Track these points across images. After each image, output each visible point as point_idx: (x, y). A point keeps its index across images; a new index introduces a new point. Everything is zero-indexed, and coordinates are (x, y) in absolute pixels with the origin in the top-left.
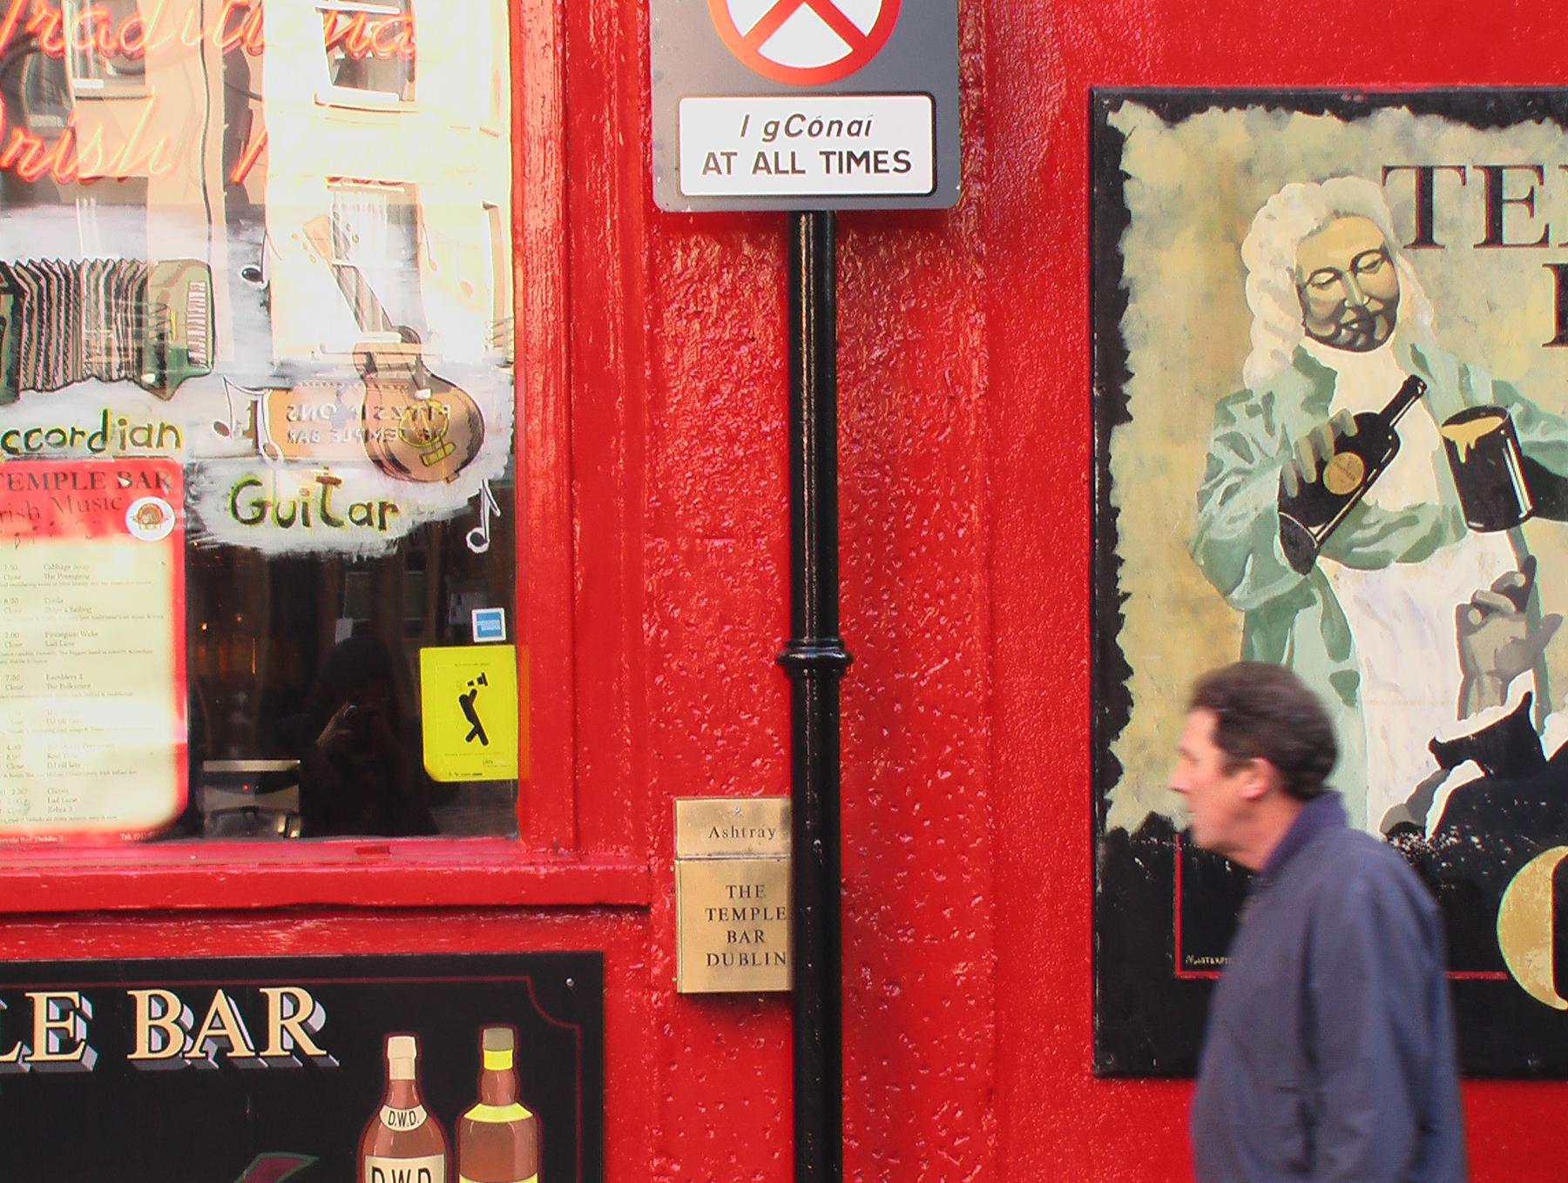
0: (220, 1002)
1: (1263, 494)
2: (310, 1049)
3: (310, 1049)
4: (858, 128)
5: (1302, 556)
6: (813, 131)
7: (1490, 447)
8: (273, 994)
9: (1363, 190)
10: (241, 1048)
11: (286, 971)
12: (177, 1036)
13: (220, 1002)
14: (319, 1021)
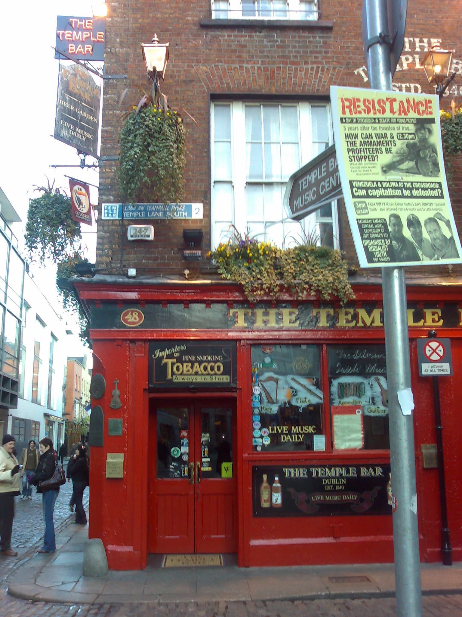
0: (371, 469)
2: (381, 474)
3: (381, 474)
4: (441, 367)
6: (437, 367)
8: (376, 468)
10: (373, 474)
11: (378, 465)
12: (366, 473)
13: (371, 469)
14: (382, 471)
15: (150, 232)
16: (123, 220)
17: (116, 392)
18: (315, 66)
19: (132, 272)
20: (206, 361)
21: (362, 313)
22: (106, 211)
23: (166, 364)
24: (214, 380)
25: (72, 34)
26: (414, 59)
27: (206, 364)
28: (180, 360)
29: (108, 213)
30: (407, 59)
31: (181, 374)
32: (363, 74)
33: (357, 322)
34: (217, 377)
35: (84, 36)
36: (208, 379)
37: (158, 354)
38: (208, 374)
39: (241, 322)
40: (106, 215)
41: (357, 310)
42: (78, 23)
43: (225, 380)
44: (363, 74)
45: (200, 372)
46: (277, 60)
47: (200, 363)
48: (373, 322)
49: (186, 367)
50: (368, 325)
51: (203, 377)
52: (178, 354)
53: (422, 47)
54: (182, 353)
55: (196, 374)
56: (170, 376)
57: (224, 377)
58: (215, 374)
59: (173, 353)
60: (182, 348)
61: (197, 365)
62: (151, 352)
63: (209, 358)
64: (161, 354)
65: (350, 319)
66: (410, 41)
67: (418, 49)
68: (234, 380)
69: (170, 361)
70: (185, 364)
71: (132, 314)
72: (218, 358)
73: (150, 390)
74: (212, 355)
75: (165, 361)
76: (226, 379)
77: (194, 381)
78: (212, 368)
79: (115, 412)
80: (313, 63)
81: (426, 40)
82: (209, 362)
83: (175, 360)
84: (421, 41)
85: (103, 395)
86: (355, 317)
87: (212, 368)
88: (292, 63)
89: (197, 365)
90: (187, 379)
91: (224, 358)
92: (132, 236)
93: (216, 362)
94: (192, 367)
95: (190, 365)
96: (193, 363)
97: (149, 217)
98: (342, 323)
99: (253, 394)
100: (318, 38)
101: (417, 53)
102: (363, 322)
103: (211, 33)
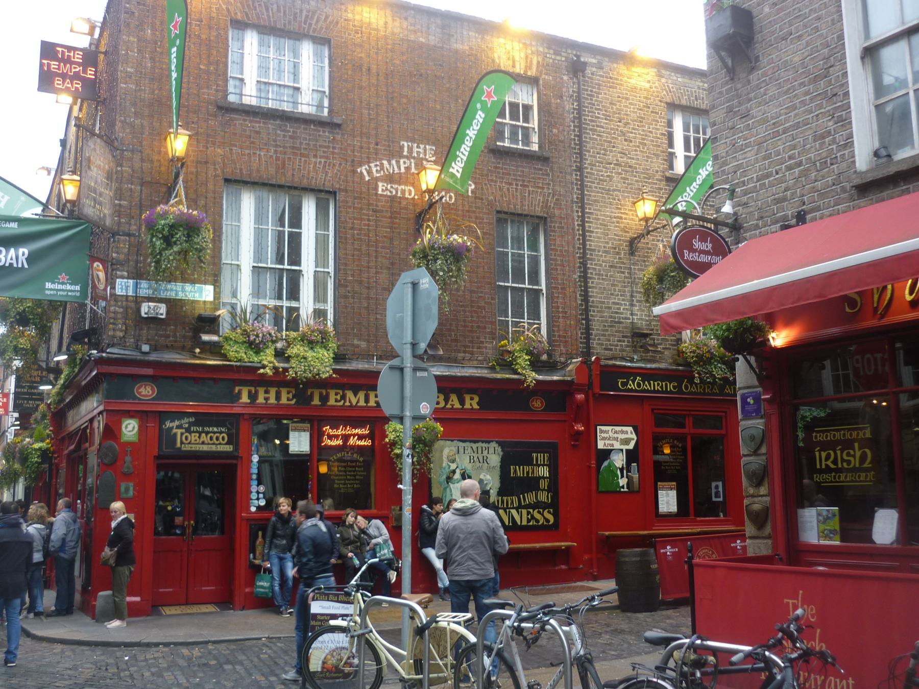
1: (445, 477)
5: (448, 483)
7: (464, 473)
9: (453, 448)
15: (162, 310)
16: (136, 297)
17: (128, 459)
18: (323, 160)
19: (146, 348)
20: (212, 432)
21: (350, 394)
22: (120, 287)
23: (175, 434)
24: (219, 449)
25: (59, 66)
26: (411, 163)
27: (212, 435)
28: (188, 430)
29: (122, 289)
30: (405, 163)
31: (189, 443)
32: (365, 173)
33: (345, 402)
34: (222, 446)
35: (73, 70)
36: (214, 448)
37: (168, 424)
38: (214, 444)
39: (245, 399)
40: (120, 290)
41: (346, 391)
42: (67, 54)
43: (228, 450)
44: (365, 173)
45: (206, 442)
46: (289, 150)
47: (207, 433)
48: (358, 402)
49: (194, 437)
50: (354, 404)
51: (210, 446)
52: (187, 426)
53: (418, 153)
54: (191, 424)
55: (203, 443)
56: (178, 445)
57: (228, 446)
58: (220, 444)
59: (182, 425)
60: (192, 420)
61: (203, 435)
62: (161, 423)
63: (215, 429)
64: (171, 425)
65: (339, 399)
66: (408, 145)
67: (415, 154)
68: (236, 449)
69: (179, 431)
70: (193, 434)
71: (145, 387)
72: (223, 430)
73: (158, 457)
74: (217, 426)
75: (175, 431)
76: (229, 448)
77: (201, 449)
78: (217, 439)
79: (127, 476)
80: (321, 157)
81: (422, 146)
82: (215, 433)
83: (183, 431)
84: (418, 147)
85: (116, 461)
86: (343, 397)
87: (217, 439)
88: (302, 155)
89: (203, 435)
90: (195, 448)
91: (229, 429)
92: (146, 314)
93: (221, 433)
94: (199, 437)
95: (198, 435)
96: (200, 433)
97: (163, 295)
98: (332, 402)
99: (252, 461)
100: (326, 134)
101: (414, 158)
102: (350, 402)
103: (227, 117)
